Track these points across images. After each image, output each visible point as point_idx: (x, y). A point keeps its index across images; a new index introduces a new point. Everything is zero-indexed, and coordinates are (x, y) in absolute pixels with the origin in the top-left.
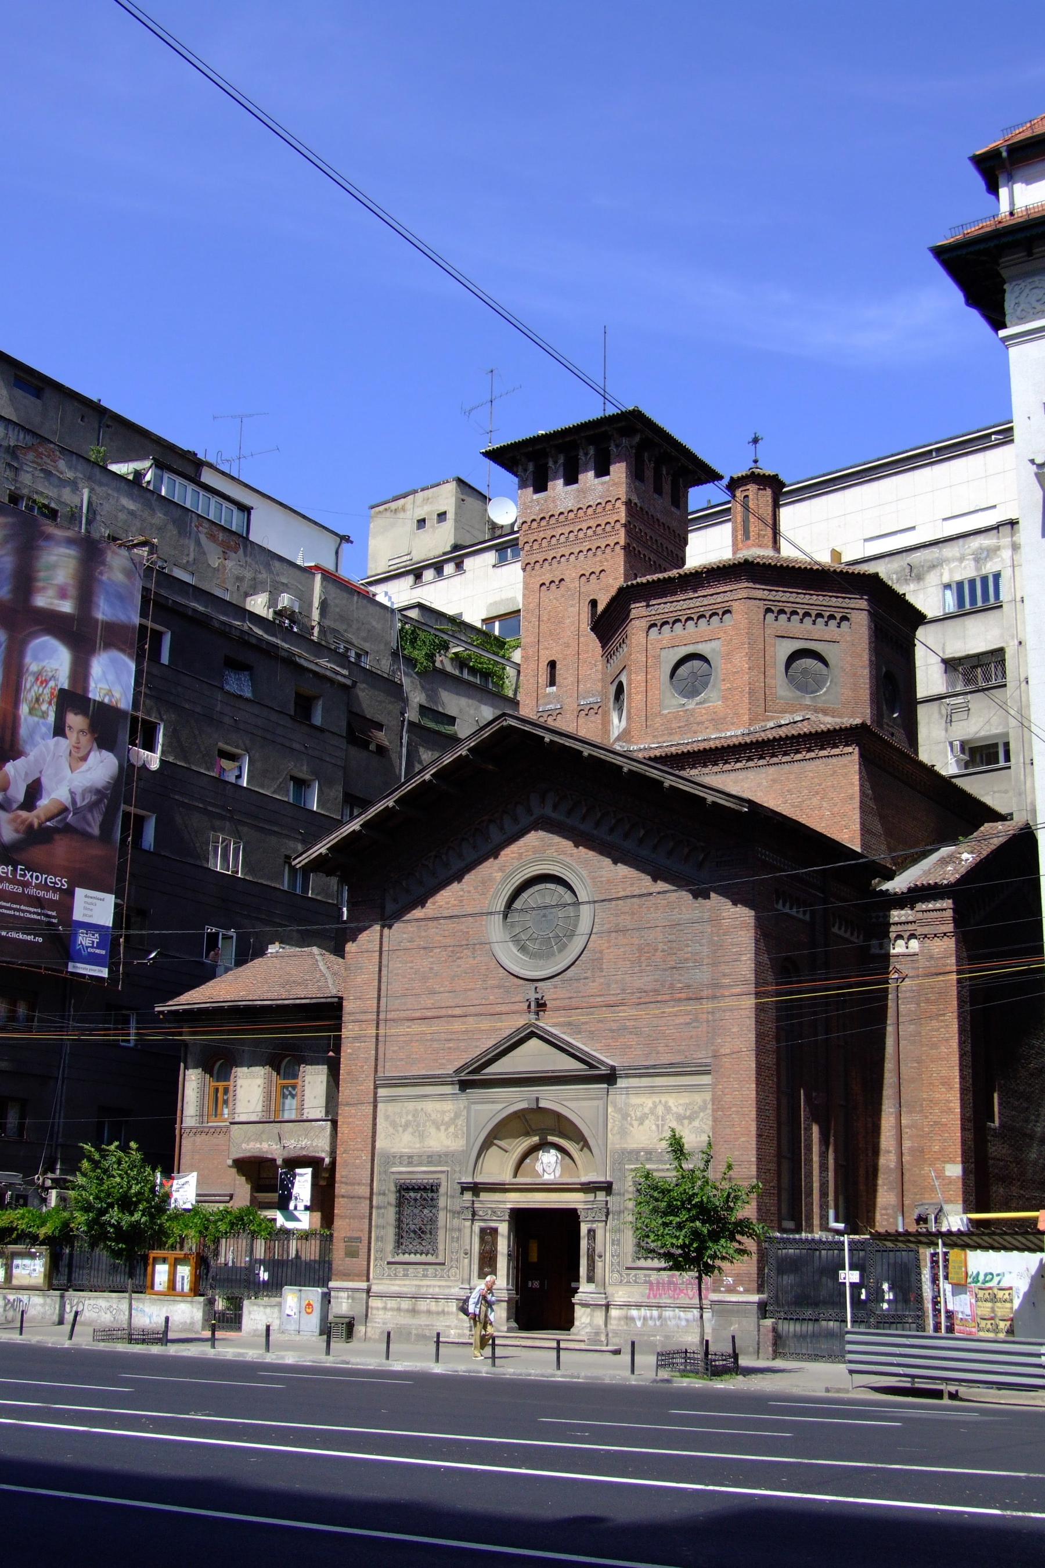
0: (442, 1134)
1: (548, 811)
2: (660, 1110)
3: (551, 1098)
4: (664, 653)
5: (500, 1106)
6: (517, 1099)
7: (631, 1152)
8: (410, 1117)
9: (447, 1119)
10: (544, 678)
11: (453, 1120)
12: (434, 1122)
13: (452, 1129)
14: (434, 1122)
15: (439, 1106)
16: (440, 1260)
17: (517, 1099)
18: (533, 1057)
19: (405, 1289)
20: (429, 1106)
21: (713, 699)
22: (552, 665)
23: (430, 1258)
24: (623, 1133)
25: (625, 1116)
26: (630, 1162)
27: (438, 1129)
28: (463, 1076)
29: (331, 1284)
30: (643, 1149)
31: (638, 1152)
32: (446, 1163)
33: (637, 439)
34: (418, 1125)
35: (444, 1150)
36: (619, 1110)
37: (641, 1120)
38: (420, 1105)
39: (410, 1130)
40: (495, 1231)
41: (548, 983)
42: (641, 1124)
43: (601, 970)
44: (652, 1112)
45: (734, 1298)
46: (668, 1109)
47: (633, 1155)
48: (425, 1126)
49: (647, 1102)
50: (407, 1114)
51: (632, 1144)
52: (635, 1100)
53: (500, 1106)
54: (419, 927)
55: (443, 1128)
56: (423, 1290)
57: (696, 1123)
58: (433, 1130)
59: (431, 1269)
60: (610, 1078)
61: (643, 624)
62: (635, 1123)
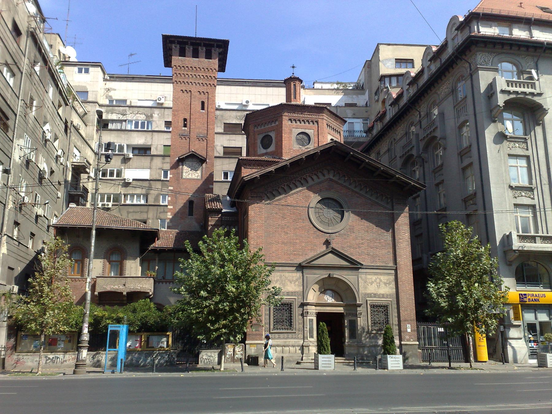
0: (293, 285)
1: (331, 177)
2: (378, 281)
3: (337, 274)
5: (318, 276)
6: (324, 274)
7: (368, 294)
8: (278, 278)
9: (294, 279)
11: (297, 280)
12: (289, 280)
13: (297, 283)
14: (289, 280)
15: (290, 274)
16: (294, 331)
17: (324, 274)
18: (331, 259)
19: (279, 343)
20: (287, 274)
21: (296, 147)
22: (185, 120)
23: (289, 331)
24: (366, 288)
25: (365, 282)
26: (368, 297)
27: (291, 282)
28: (304, 264)
29: (247, 342)
30: (373, 293)
31: (371, 294)
32: (295, 295)
33: (221, 50)
34: (282, 281)
35: (294, 290)
36: (363, 280)
37: (372, 283)
38: (282, 274)
39: (279, 282)
40: (312, 320)
41: (334, 235)
42: (371, 285)
43: (354, 232)
44: (375, 281)
45: (411, 343)
46: (381, 280)
47: (370, 295)
48: (285, 281)
49: (374, 278)
50: (277, 276)
51: (369, 291)
52: (369, 277)
53: (318, 276)
54: (279, 209)
55: (293, 282)
56: (287, 343)
57: (391, 286)
58: (289, 283)
59: (290, 335)
60: (358, 269)
61: (287, 118)
62: (369, 284)
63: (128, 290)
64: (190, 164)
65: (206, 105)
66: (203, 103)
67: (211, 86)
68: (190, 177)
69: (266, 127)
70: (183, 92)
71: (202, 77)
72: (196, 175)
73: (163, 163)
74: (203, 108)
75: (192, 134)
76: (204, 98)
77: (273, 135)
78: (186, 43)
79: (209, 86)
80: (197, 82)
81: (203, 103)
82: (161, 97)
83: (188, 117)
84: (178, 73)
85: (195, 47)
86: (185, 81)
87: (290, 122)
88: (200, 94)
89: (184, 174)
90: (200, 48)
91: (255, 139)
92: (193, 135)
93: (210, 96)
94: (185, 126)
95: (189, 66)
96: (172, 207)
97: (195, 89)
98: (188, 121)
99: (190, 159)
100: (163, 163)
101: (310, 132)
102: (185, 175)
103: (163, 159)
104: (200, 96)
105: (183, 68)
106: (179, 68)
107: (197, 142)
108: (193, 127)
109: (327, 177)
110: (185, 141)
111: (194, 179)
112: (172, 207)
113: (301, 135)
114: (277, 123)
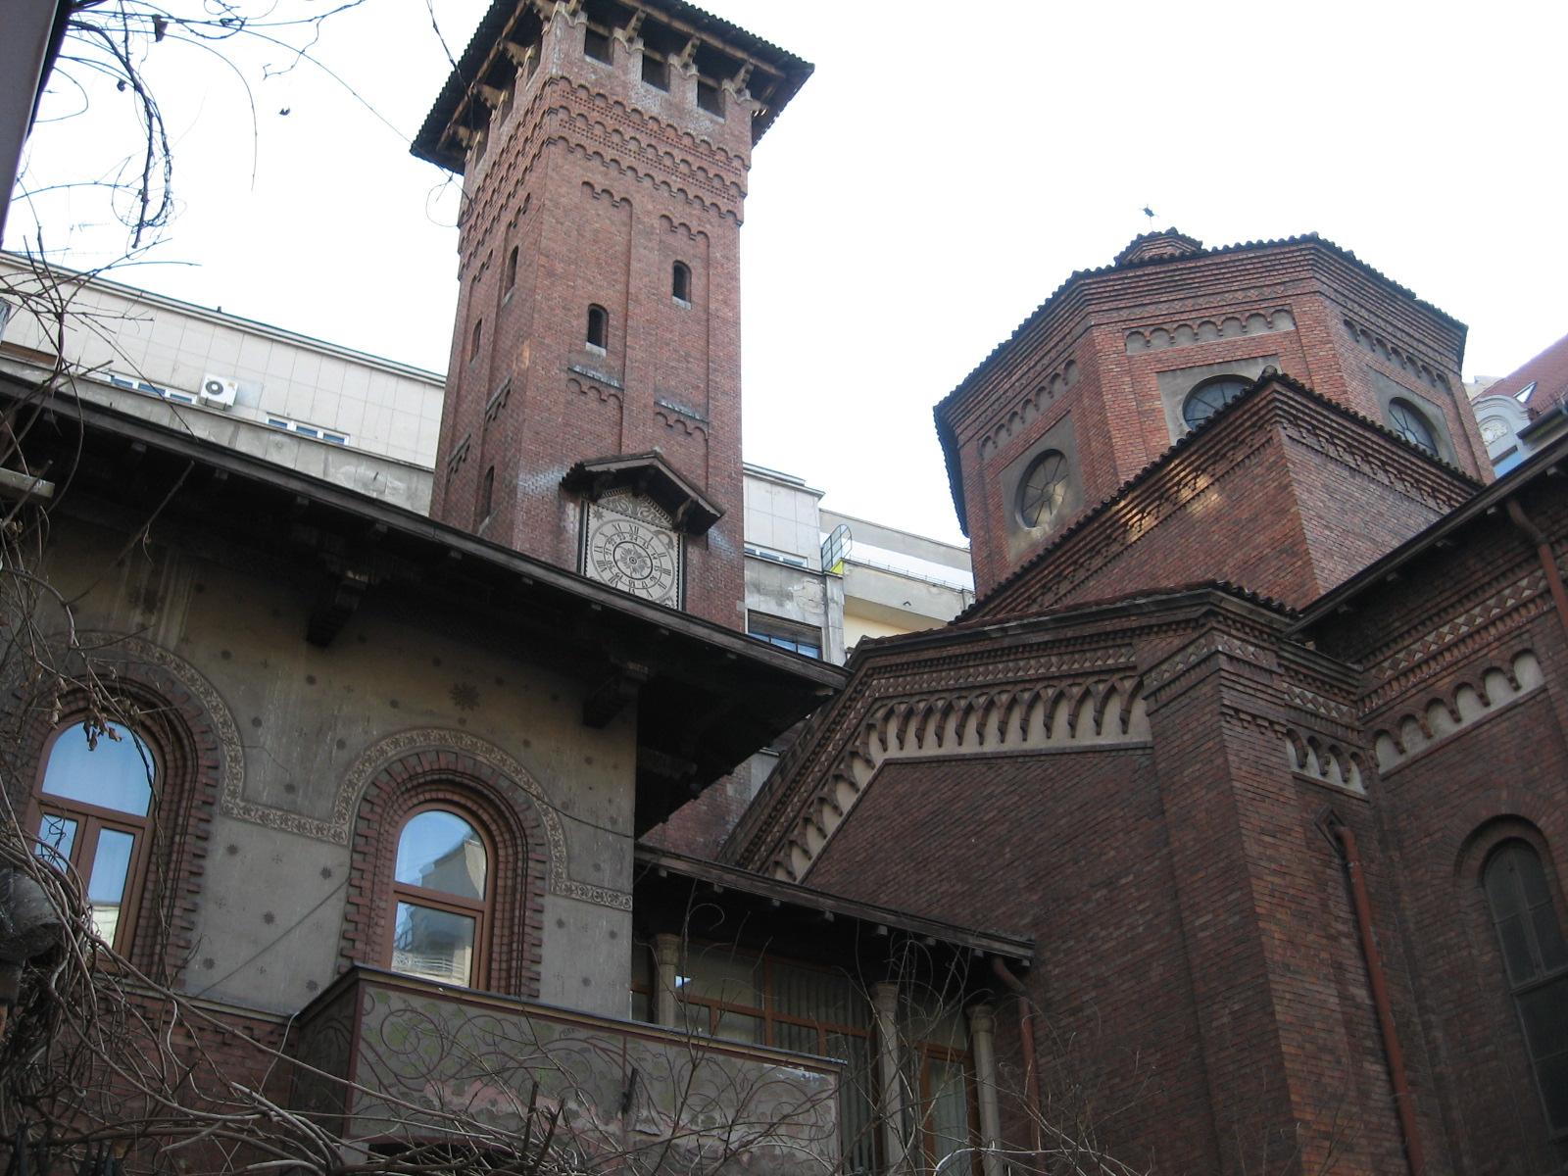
10: (582, 324)
22: (597, 317)
64: (625, 527)
65: (696, 283)
76: (684, 248)
80: (659, 177)
82: (224, 383)
83: (609, 298)
84: (576, 109)
88: (673, 229)
94: (595, 335)
97: (648, 203)
99: (624, 502)
104: (670, 239)
110: (594, 405)
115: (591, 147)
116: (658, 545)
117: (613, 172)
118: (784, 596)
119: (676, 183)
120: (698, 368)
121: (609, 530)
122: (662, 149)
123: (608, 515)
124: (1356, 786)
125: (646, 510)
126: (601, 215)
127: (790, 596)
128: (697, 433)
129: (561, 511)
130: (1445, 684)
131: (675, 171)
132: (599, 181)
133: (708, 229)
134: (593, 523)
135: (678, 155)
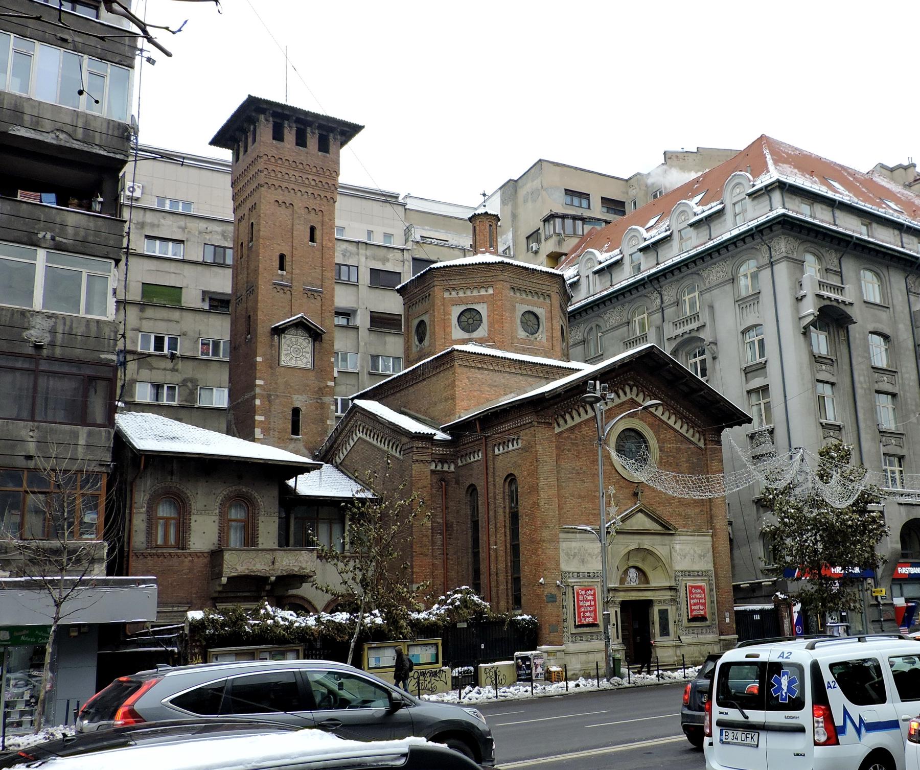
4: (517, 305)
10: (276, 264)
22: (282, 257)
63: (279, 573)
64: (293, 340)
65: (318, 234)
66: (312, 229)
67: (328, 201)
68: (292, 363)
69: (468, 293)
70: (280, 206)
71: (313, 183)
72: (305, 360)
73: (141, 319)
74: (312, 239)
75: (295, 284)
76: (314, 220)
77: (482, 309)
78: (287, 117)
79: (325, 200)
80: (303, 190)
81: (312, 229)
84: (271, 168)
85: (324, 133)
86: (284, 185)
87: (512, 294)
89: (283, 358)
90: (286, 123)
91: (447, 313)
92: (298, 287)
93: (326, 219)
94: (282, 268)
95: (291, 159)
96: (262, 418)
98: (288, 259)
99: (293, 331)
100: (141, 319)
101: (539, 311)
102: (284, 360)
103: (142, 311)
105: (280, 162)
106: (273, 160)
107: (305, 300)
108: (298, 271)
109: (629, 396)
111: (300, 369)
112: (262, 418)
113: (527, 316)
114: (491, 291)
115: (277, 183)
116: (305, 343)
117: (286, 193)
118: (385, 260)
119: (310, 190)
120: (318, 271)
121: (288, 342)
122: (304, 176)
123: (288, 336)
124: (452, 468)
125: (300, 332)
126: (283, 214)
127: (388, 260)
128: (319, 298)
129: (273, 340)
130: (469, 451)
131: (309, 185)
132: (281, 200)
133: (323, 208)
134: (283, 340)
135: (310, 177)
